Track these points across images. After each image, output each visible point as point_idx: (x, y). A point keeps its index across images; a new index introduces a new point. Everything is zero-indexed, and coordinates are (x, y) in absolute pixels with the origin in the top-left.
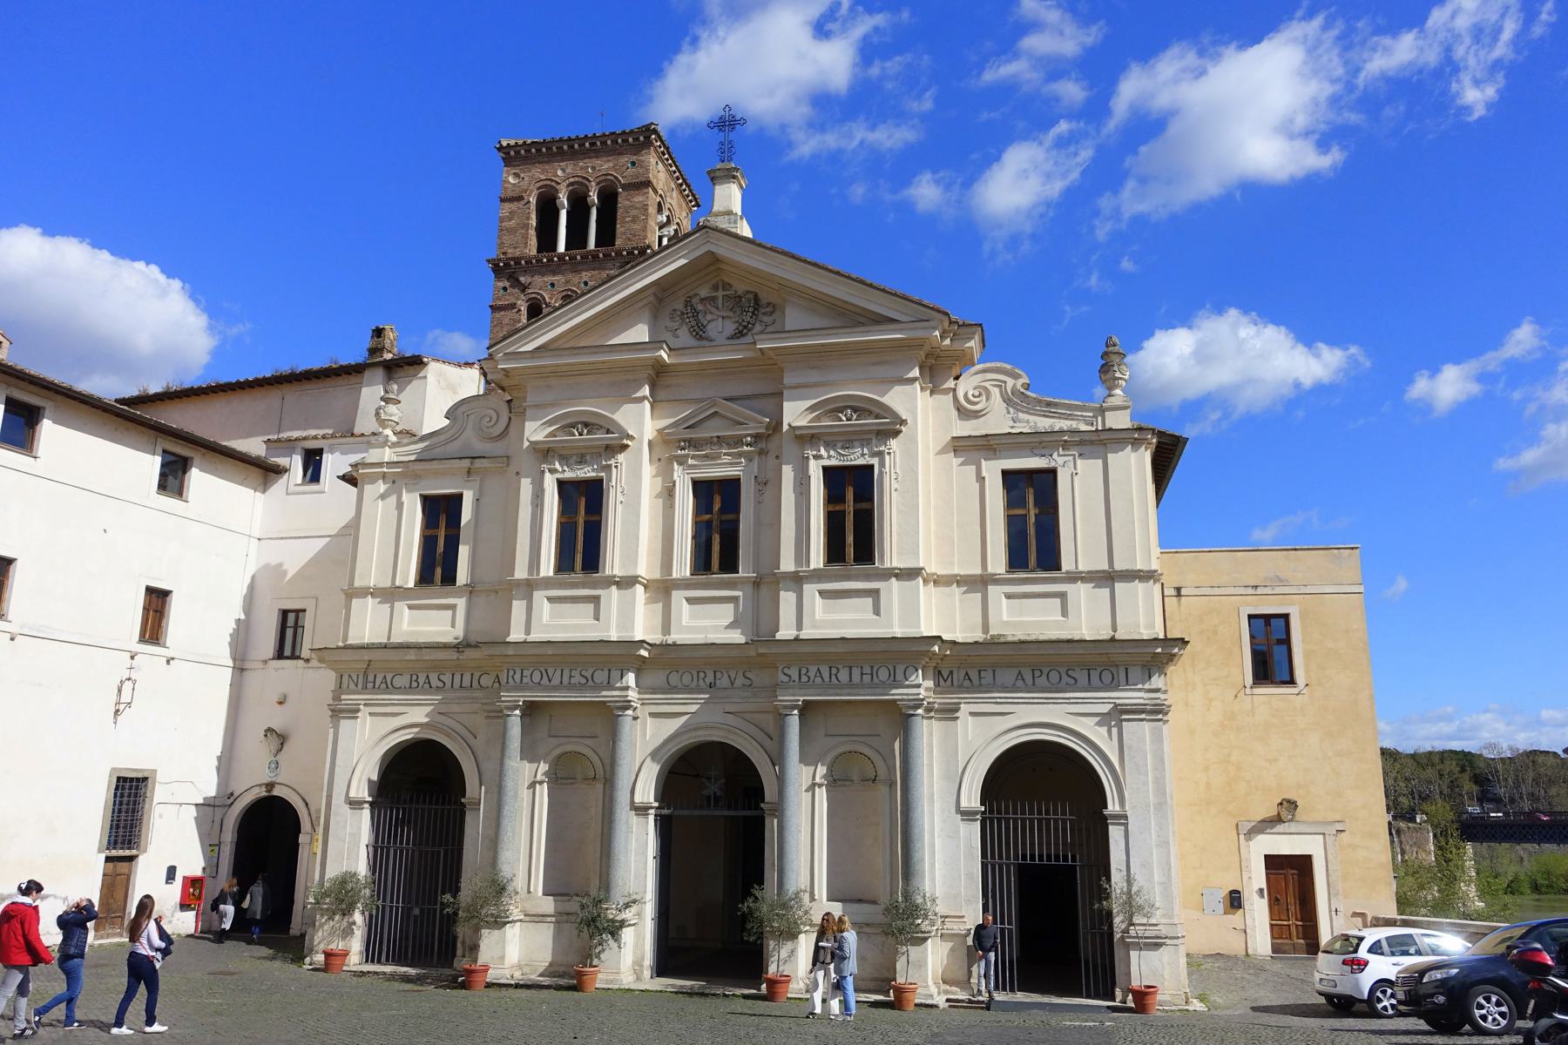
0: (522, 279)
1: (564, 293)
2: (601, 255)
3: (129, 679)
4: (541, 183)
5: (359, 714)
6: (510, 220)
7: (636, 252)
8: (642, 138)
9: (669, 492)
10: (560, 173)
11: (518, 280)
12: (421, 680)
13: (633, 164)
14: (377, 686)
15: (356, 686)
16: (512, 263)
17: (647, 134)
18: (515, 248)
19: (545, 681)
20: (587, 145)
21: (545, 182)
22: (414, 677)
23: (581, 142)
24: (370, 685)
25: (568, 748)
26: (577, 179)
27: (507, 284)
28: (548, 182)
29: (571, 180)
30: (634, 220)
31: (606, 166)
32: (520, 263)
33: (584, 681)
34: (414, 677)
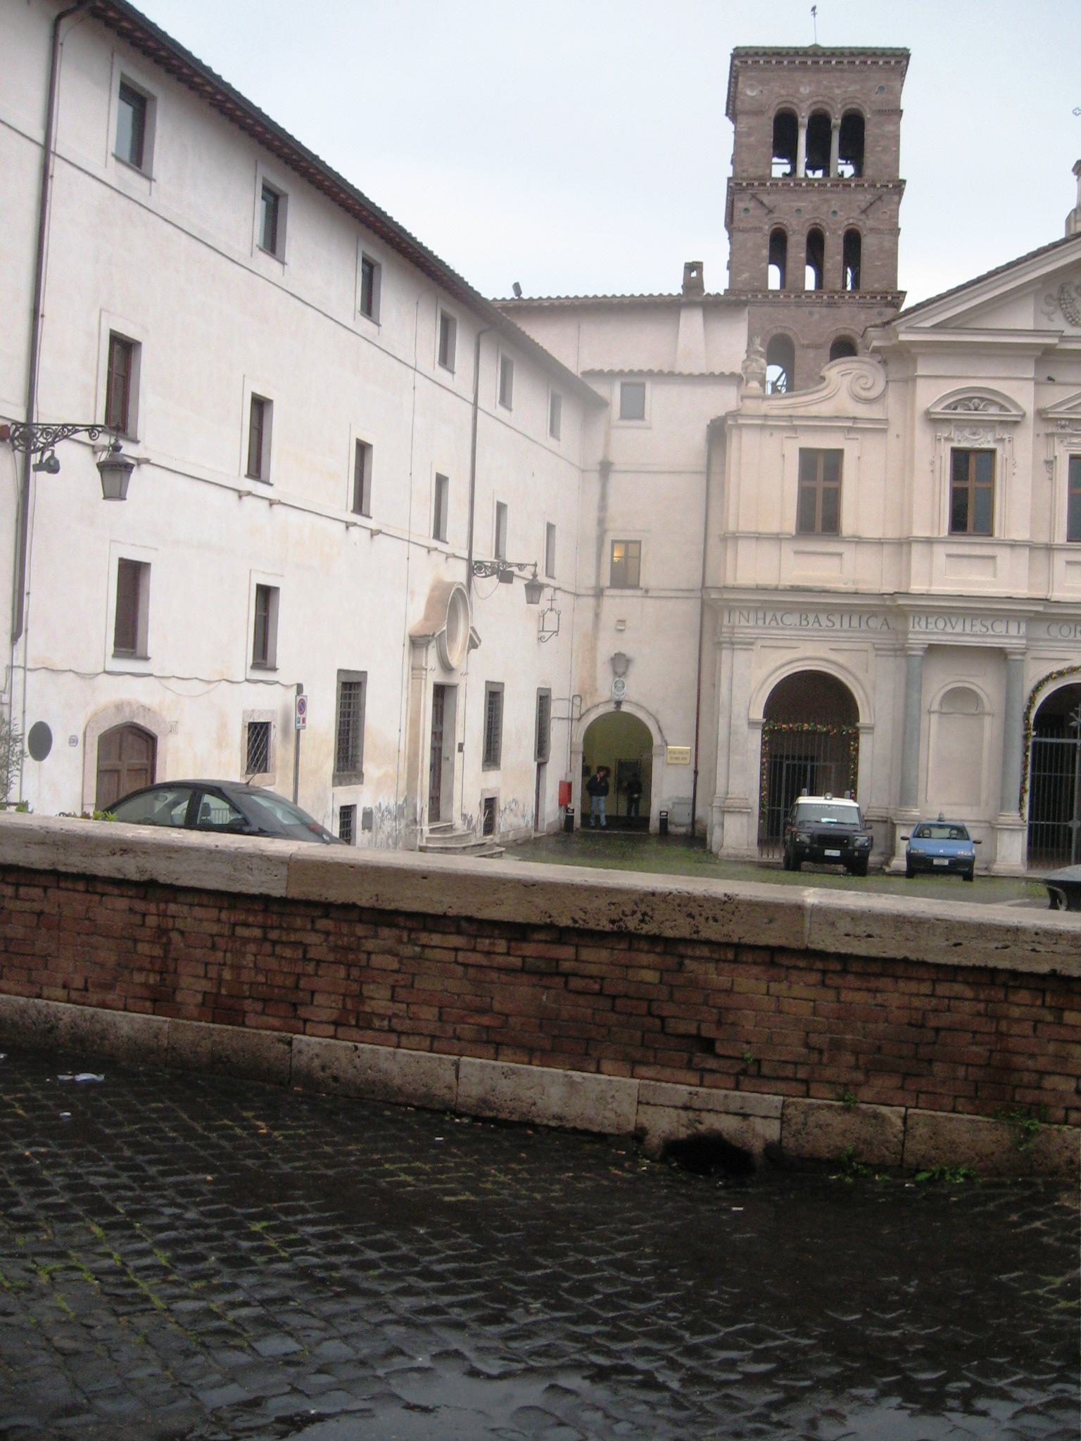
0: (766, 199)
1: (812, 221)
2: (853, 185)
3: (551, 610)
4: (781, 99)
5: (754, 647)
6: (749, 135)
7: (891, 186)
8: (893, 63)
9: (1050, 463)
10: (802, 89)
11: (762, 203)
12: (811, 619)
13: (882, 88)
14: (767, 622)
15: (748, 621)
16: (756, 184)
17: (898, 59)
18: (756, 167)
19: (949, 629)
20: (834, 62)
21: (784, 99)
22: (804, 617)
23: (828, 59)
24: (760, 622)
25: (960, 685)
26: (820, 99)
27: (751, 205)
28: (791, 99)
29: (815, 99)
30: (885, 150)
31: (851, 88)
32: (765, 185)
33: (984, 630)
34: (804, 617)
